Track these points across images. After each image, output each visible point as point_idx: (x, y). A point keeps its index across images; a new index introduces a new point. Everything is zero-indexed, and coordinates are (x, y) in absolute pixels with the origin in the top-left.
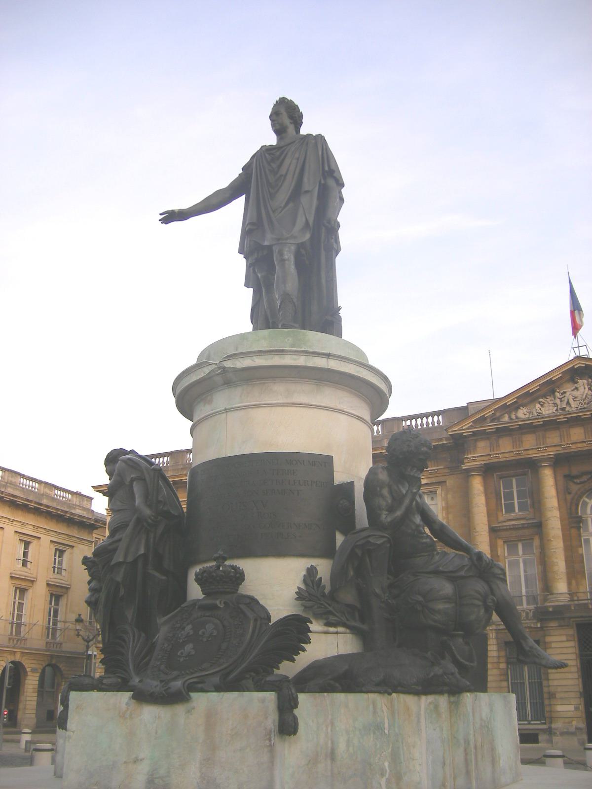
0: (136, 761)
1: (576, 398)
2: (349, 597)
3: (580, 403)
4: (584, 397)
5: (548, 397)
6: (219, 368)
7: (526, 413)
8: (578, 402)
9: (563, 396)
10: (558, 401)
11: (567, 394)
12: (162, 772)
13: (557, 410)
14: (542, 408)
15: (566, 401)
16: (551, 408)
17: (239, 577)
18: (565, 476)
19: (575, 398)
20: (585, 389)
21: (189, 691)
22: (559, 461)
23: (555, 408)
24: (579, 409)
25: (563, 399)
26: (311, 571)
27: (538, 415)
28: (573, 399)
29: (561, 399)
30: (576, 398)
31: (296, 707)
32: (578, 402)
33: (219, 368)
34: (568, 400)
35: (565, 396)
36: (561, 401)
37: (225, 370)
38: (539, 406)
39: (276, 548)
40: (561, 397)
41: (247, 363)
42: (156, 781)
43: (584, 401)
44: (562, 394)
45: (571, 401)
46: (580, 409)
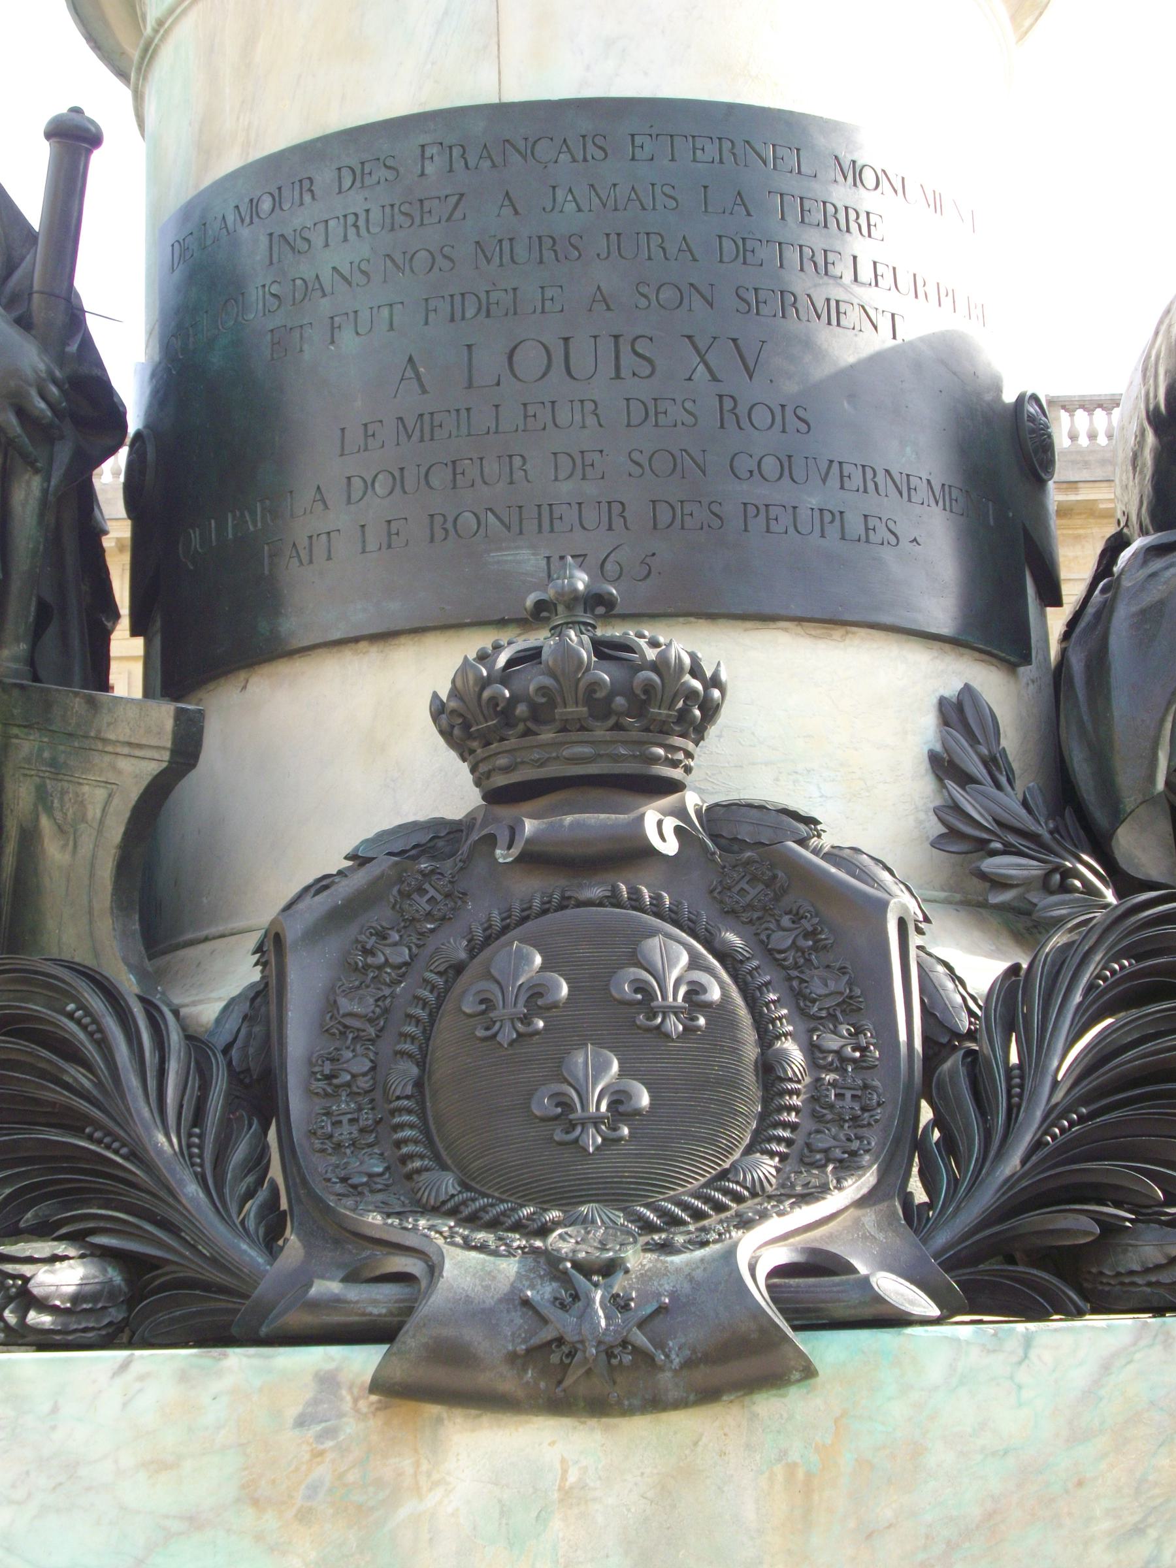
26: (958, 713)
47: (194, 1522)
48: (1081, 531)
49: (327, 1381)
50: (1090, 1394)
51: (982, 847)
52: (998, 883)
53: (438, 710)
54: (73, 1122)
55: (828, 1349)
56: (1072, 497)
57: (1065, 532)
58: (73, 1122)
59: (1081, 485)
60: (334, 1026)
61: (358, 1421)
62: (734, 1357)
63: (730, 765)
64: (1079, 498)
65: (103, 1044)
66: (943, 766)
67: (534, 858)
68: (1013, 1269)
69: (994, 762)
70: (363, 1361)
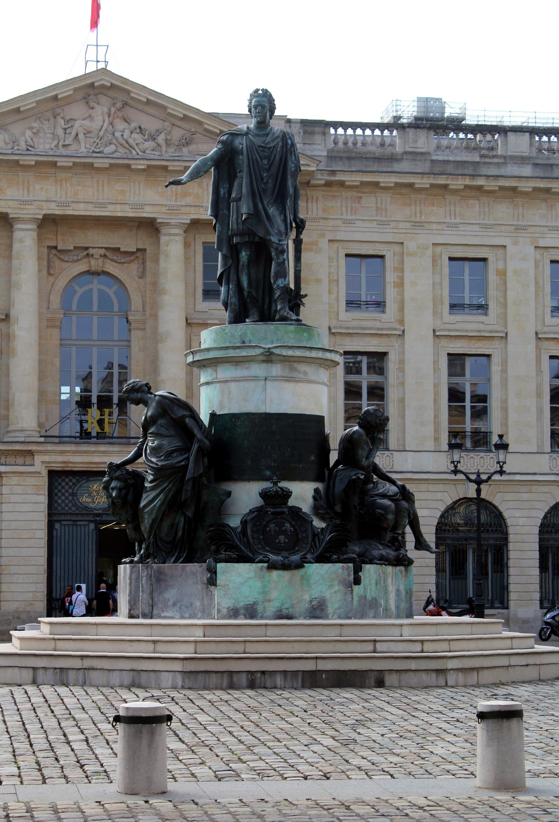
0: (269, 601)
1: (90, 132)
2: (338, 508)
3: (95, 142)
4: (101, 133)
5: (44, 122)
6: (267, 352)
7: (7, 141)
8: (92, 140)
9: (70, 125)
10: (60, 132)
11: (77, 124)
12: (286, 606)
13: (57, 146)
14: (34, 139)
15: (73, 134)
16: (51, 141)
17: (287, 494)
18: (50, 248)
19: (87, 133)
20: (104, 122)
21: (216, 563)
22: (48, 223)
23: (55, 142)
24: (91, 151)
25: (68, 131)
26: (316, 491)
27: (28, 150)
28: (84, 134)
29: (65, 129)
30: (90, 132)
31: (361, 571)
32: (92, 140)
33: (267, 352)
34: (77, 135)
35: (72, 126)
36: (65, 133)
37: (272, 354)
38: (31, 133)
39: (302, 478)
40: (66, 127)
41: (290, 353)
42: (283, 610)
43: (101, 140)
44: (68, 121)
45: (81, 136)
46: (94, 152)
47: (250, 578)
48: (336, 194)
49: (262, 566)
50: (328, 570)
51: (318, 509)
52: (320, 514)
53: (260, 494)
54: (229, 540)
55: (306, 565)
56: (333, 178)
57: (328, 193)
58: (229, 540)
59: (337, 172)
60: (253, 531)
61: (265, 570)
62: (299, 566)
63: (292, 502)
64: (337, 178)
65: (231, 532)
66: (314, 498)
67: (273, 513)
68: (321, 559)
69: (320, 497)
70: (266, 565)
